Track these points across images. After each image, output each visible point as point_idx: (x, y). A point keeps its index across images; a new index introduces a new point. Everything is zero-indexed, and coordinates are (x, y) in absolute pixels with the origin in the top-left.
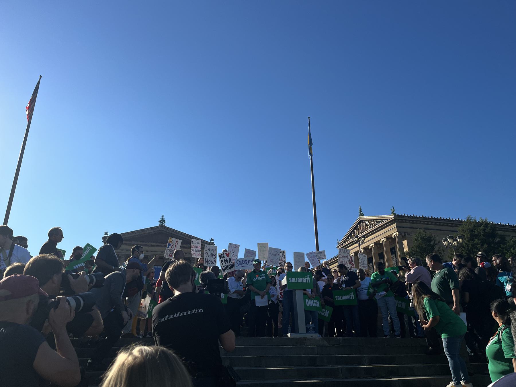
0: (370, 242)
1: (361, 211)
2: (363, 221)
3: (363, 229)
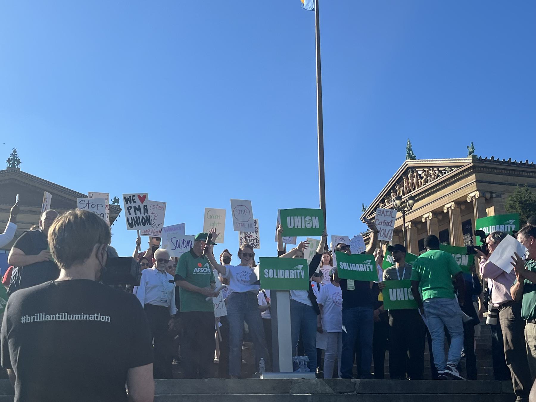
0: (423, 210)
1: (410, 150)
2: (412, 169)
3: (413, 184)
